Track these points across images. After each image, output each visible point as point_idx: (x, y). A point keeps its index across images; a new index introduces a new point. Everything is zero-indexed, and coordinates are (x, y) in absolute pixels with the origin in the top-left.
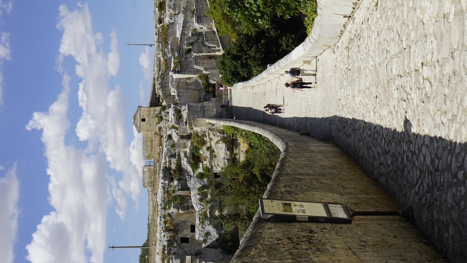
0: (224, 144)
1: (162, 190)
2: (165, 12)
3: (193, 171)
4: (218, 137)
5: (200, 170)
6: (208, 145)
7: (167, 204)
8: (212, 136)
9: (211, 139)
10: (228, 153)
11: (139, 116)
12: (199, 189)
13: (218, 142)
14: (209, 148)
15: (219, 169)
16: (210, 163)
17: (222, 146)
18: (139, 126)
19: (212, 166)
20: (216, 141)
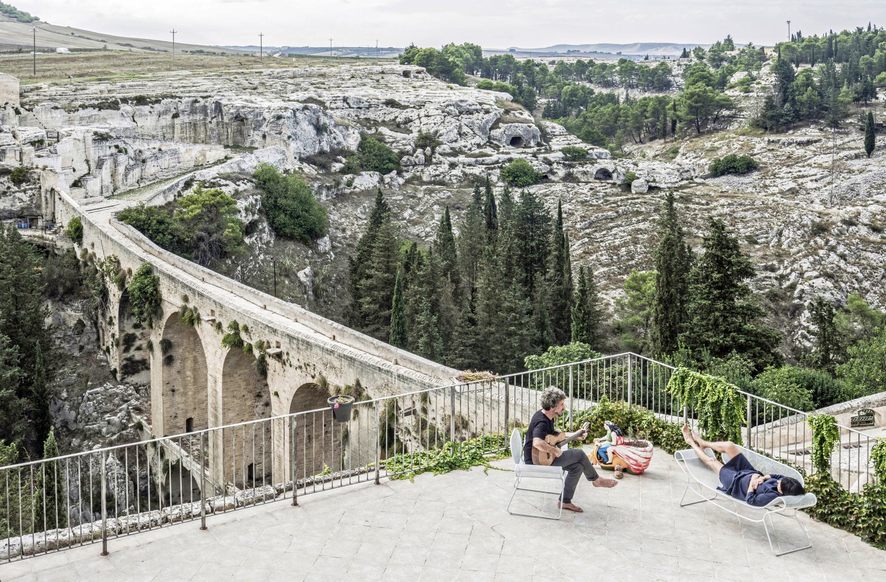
2: (136, 105)
8: (30, 193)
13: (21, 200)
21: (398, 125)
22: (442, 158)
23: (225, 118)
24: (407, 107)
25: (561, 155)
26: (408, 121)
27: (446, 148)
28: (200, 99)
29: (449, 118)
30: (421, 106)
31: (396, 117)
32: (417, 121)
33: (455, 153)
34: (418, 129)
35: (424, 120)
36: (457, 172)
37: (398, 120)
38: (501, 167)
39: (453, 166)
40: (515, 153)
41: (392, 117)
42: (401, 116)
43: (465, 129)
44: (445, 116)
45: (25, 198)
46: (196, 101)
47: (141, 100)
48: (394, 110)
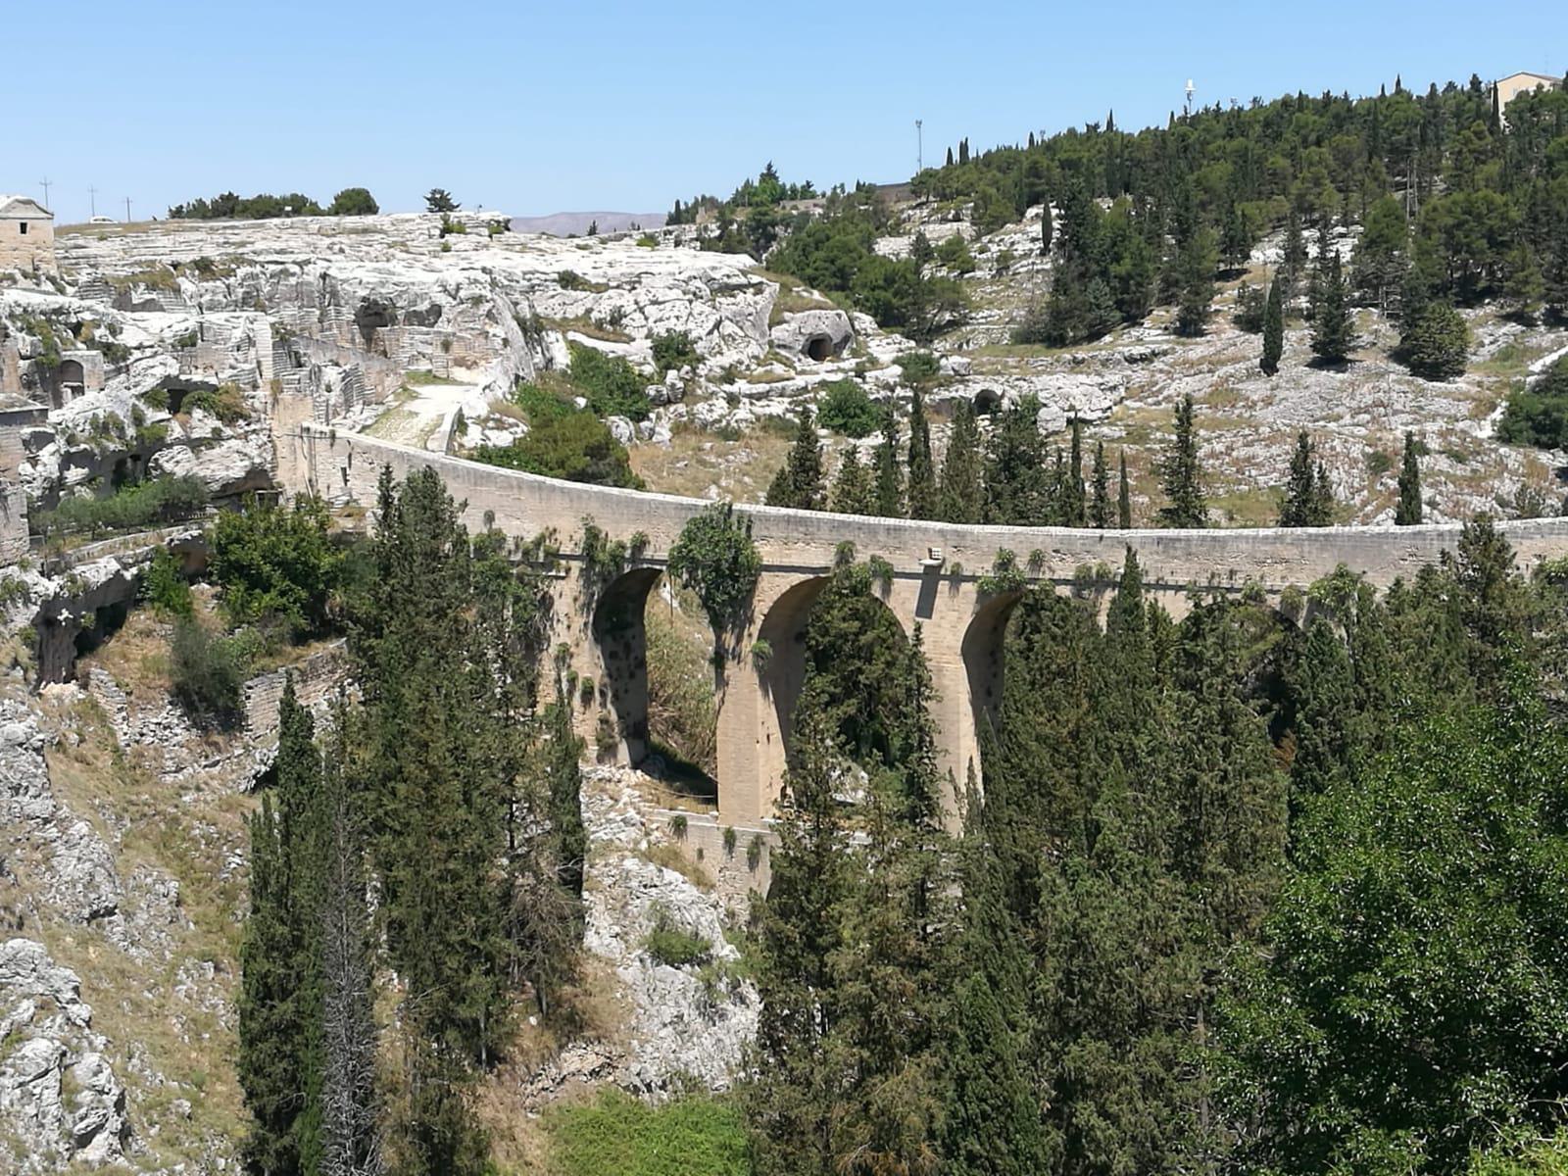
0: (243, 474)
1: (52, 306)
3: (142, 395)
4: (260, 455)
5: (152, 415)
6: (228, 431)
7: (26, 319)
9: (245, 437)
10: (216, 487)
11: (33, 215)
12: (112, 415)
14: (216, 431)
15: (168, 467)
16: (178, 441)
17: (238, 470)
18: (11, 215)
19: (170, 446)
20: (247, 450)
21: (599, 324)
22: (712, 387)
23: (344, 310)
24: (607, 287)
25: (898, 370)
26: (617, 317)
27: (714, 364)
28: (295, 269)
29: (698, 306)
30: (634, 284)
31: (589, 311)
32: (637, 315)
33: (729, 375)
34: (645, 331)
35: (650, 310)
36: (743, 412)
37: (594, 315)
38: (815, 400)
39: (733, 400)
40: (824, 371)
41: (581, 312)
42: (603, 308)
43: (728, 328)
44: (691, 302)
45: (251, 449)
46: (286, 273)
47: (204, 267)
48: (580, 294)
